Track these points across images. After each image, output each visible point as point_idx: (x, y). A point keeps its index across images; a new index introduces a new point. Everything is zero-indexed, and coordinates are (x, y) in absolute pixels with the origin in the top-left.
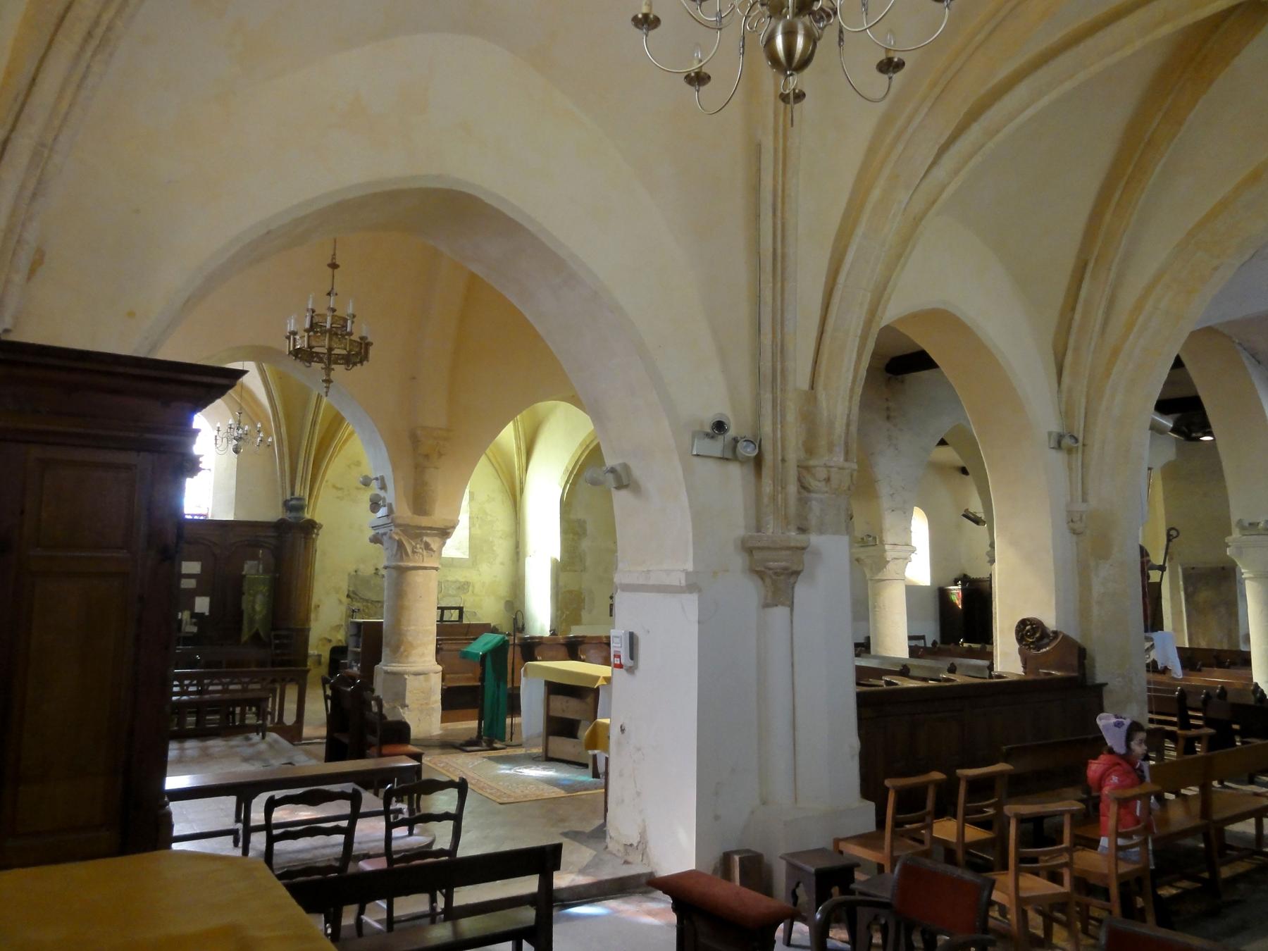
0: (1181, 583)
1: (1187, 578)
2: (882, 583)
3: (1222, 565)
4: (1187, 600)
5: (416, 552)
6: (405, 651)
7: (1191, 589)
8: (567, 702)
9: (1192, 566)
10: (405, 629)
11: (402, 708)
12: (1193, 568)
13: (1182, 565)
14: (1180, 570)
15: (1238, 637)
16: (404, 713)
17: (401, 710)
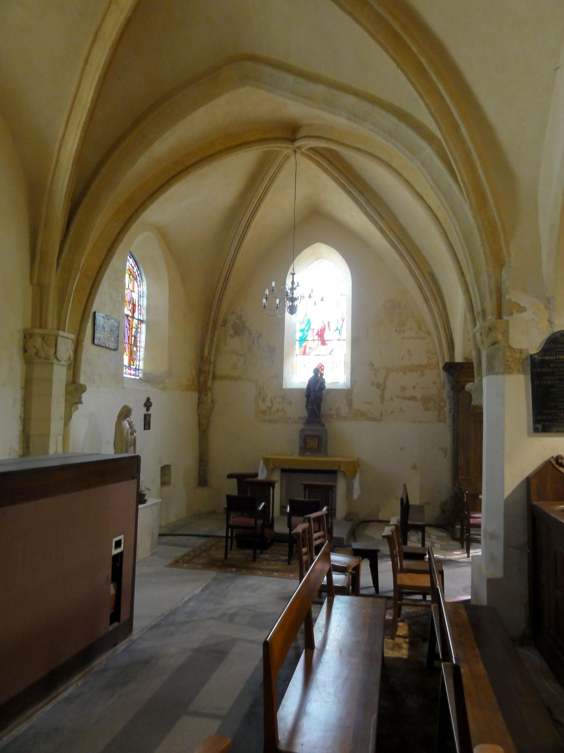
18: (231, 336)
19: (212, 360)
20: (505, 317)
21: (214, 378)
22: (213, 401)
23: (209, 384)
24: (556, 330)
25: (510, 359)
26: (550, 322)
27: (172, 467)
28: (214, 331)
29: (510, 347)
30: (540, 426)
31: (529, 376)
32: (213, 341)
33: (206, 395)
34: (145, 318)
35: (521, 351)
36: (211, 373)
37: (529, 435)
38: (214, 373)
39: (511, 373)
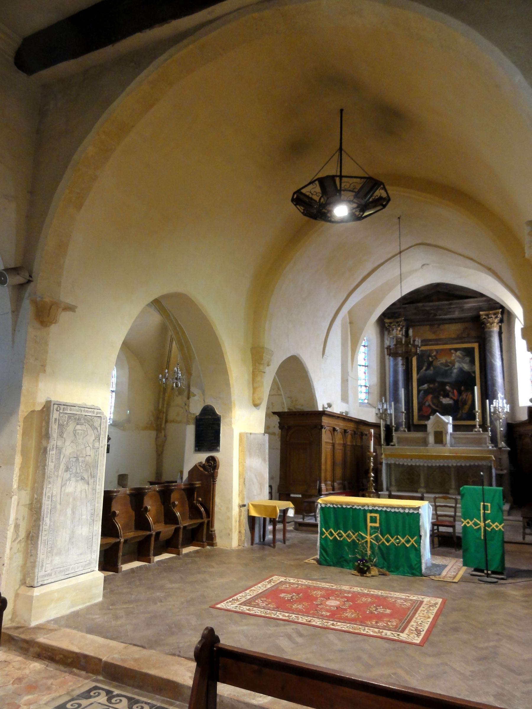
18: (177, 396)
19: (165, 410)
20: (190, 399)
21: (166, 422)
22: (165, 436)
23: (163, 426)
24: (206, 404)
25: (190, 418)
26: (204, 401)
27: (129, 477)
28: (165, 394)
29: (189, 412)
30: (197, 449)
31: (195, 425)
32: (164, 399)
33: (161, 432)
34: (115, 390)
35: (194, 414)
36: (164, 418)
37: (194, 453)
38: (166, 418)
39: (189, 424)
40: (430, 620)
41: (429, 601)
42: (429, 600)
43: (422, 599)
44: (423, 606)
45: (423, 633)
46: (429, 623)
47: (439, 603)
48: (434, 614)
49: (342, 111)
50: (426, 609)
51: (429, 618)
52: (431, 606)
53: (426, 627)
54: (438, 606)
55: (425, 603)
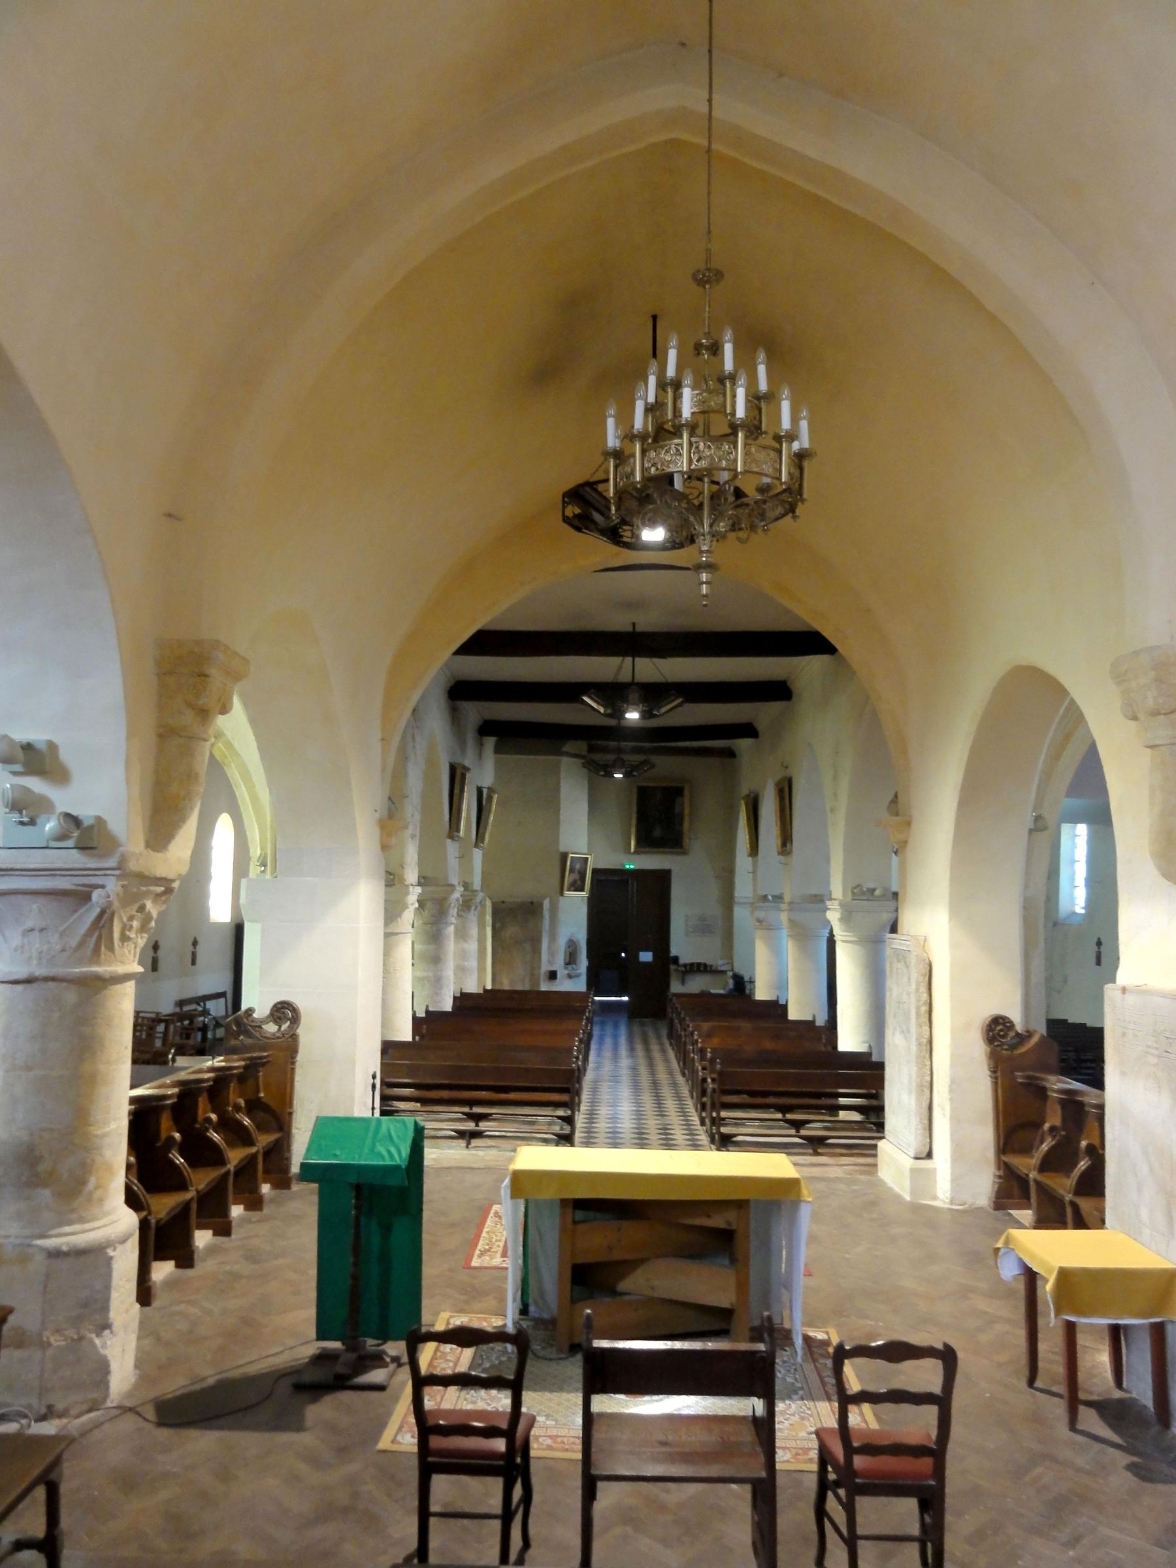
0: (489, 919)
1: (496, 913)
2: (394, 937)
3: (529, 900)
4: (493, 937)
5: (129, 939)
6: (97, 1188)
7: (498, 925)
8: (619, 1230)
9: (501, 900)
10: (99, 1132)
11: (98, 1335)
12: (503, 902)
13: (491, 899)
14: (489, 904)
15: (539, 974)
16: (104, 1346)
17: (97, 1342)
40: (485, 1230)
41: (491, 1259)
42: (494, 1260)
43: (504, 1261)
44: (500, 1250)
45: (492, 1214)
46: (486, 1226)
47: (475, 1257)
48: (482, 1239)
49: (655, 318)
50: (494, 1244)
51: (488, 1232)
52: (489, 1251)
53: (489, 1222)
54: (477, 1252)
55: (499, 1255)
